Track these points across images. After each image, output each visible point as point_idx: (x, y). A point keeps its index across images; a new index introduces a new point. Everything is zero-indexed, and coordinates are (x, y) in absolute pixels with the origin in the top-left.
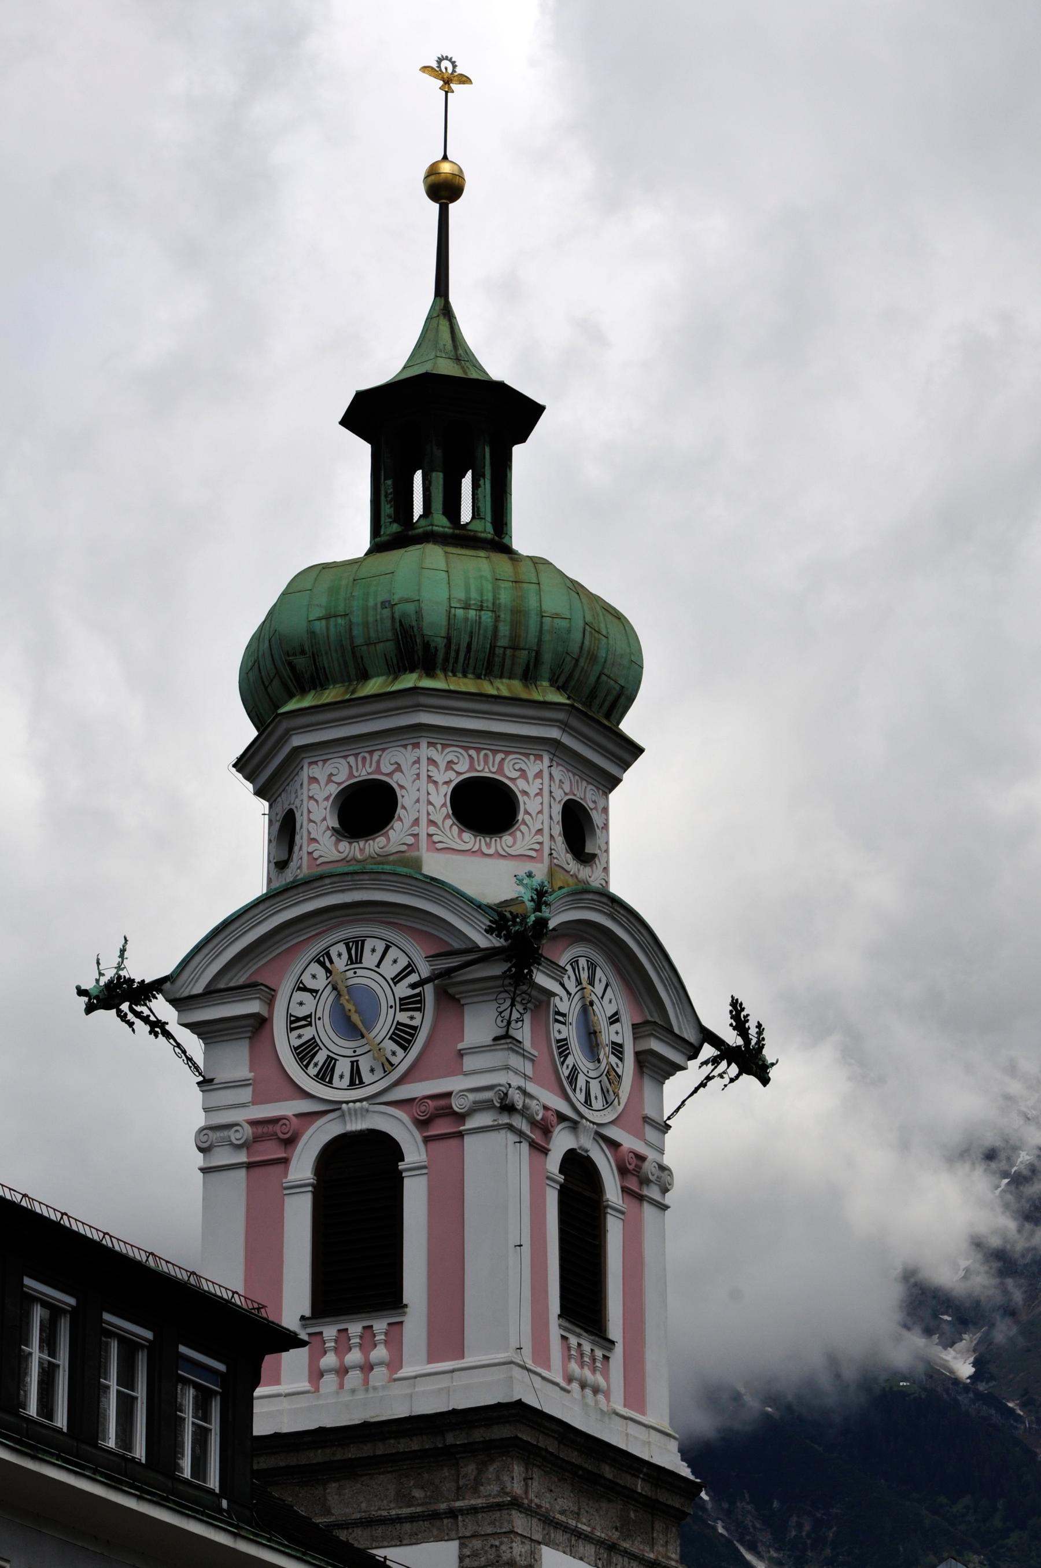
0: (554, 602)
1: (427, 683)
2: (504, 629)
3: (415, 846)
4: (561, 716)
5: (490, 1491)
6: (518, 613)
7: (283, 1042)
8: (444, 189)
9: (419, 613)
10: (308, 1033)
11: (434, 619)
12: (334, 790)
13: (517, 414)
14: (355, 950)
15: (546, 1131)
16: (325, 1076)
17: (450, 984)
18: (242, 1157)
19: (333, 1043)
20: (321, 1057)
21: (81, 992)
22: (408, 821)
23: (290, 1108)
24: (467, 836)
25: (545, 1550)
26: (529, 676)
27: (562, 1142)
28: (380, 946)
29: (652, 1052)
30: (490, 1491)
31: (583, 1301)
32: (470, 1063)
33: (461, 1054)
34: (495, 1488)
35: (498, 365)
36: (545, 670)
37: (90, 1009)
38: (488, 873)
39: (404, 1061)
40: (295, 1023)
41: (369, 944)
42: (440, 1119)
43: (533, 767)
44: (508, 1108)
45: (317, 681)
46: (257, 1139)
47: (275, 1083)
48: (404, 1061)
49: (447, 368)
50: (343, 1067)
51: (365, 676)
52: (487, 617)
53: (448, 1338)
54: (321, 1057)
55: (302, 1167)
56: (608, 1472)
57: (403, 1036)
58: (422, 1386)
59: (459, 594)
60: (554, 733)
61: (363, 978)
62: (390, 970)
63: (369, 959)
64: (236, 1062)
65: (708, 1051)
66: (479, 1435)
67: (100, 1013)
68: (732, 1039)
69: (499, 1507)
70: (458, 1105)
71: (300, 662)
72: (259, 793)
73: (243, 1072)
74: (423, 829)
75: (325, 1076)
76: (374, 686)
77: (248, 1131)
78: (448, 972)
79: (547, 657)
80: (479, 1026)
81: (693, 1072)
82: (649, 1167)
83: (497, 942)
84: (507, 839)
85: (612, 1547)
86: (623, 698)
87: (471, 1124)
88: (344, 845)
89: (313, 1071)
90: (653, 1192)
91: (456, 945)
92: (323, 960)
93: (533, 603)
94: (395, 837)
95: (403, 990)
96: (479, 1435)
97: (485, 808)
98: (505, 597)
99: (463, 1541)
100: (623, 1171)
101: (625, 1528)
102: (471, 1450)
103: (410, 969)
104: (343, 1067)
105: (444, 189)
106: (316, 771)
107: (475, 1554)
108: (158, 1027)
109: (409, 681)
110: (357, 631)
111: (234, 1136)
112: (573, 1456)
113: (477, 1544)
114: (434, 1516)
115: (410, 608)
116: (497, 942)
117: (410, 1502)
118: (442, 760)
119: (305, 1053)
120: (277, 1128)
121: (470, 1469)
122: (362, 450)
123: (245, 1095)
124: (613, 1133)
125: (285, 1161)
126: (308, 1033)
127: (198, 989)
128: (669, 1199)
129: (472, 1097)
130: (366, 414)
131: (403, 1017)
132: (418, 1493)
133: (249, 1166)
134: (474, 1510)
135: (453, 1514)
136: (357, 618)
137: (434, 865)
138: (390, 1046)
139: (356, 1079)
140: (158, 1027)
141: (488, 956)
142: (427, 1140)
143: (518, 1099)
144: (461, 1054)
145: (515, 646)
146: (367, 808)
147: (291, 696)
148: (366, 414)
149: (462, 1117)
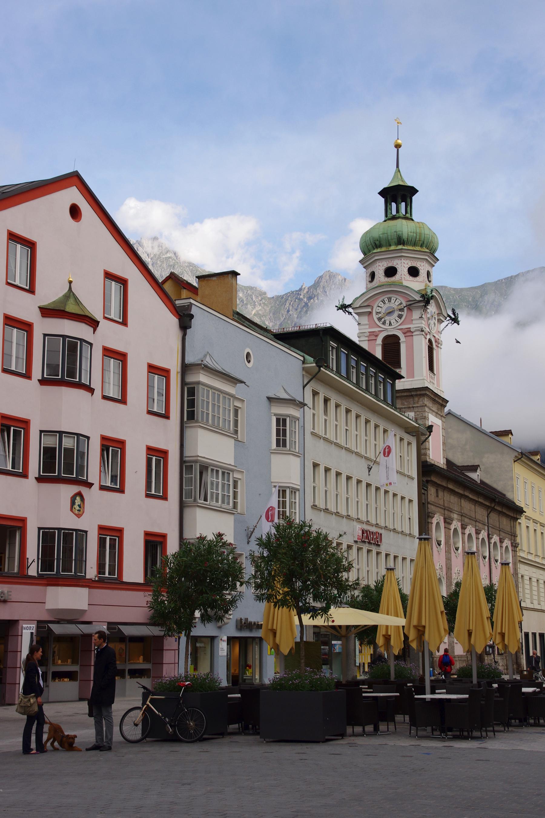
0: (427, 232)
1: (404, 248)
2: (418, 237)
3: (402, 279)
4: (428, 254)
5: (420, 403)
6: (420, 234)
7: (375, 317)
8: (398, 146)
9: (402, 234)
10: (380, 315)
12: (384, 268)
13: (413, 191)
14: (390, 299)
15: (427, 335)
16: (384, 323)
17: (411, 306)
18: (367, 339)
21: (336, 306)
22: (400, 275)
23: (377, 329)
24: (411, 277)
25: (430, 414)
26: (421, 246)
27: (428, 337)
28: (395, 299)
29: (440, 319)
30: (420, 403)
32: (414, 322)
33: (412, 320)
34: (422, 403)
35: (409, 183)
36: (425, 245)
37: (338, 310)
38: (416, 285)
39: (400, 321)
40: (377, 313)
41: (392, 298)
42: (408, 332)
43: (422, 264)
44: (422, 331)
45: (380, 246)
46: (370, 335)
47: (372, 324)
48: (400, 321)
49: (401, 183)
50: (388, 322)
51: (390, 246)
52: (415, 235)
53: (411, 374)
55: (379, 341)
56: (437, 399)
58: (406, 383)
59: (410, 230)
60: (427, 258)
62: (397, 303)
63: (393, 301)
64: (365, 320)
65: (448, 318)
66: (419, 393)
67: (340, 310)
68: (453, 316)
69: (423, 406)
70: (412, 330)
71: (377, 243)
72: (364, 267)
73: (367, 322)
74: (403, 276)
75: (384, 323)
76: (393, 248)
77: (368, 334)
78: (410, 305)
79: (425, 242)
80: (416, 314)
81: (446, 323)
82: (440, 341)
83: (421, 299)
84: (418, 278)
85: (437, 413)
86: (435, 251)
87: (414, 334)
89: (381, 322)
90: (439, 345)
91: (411, 299)
93: (423, 232)
94: (396, 278)
96: (419, 393)
97: (414, 272)
98: (418, 231)
99: (415, 412)
100: (436, 342)
101: (438, 409)
102: (416, 395)
103: (401, 304)
104: (388, 322)
105: (398, 146)
106: (380, 264)
107: (418, 415)
108: (350, 313)
109: (400, 247)
110: (389, 237)
111: (366, 335)
112: (432, 396)
113: (418, 413)
114: (409, 408)
115: (401, 233)
116: (421, 299)
117: (404, 405)
118: (406, 262)
119: (380, 319)
120: (374, 333)
121: (416, 399)
122: (383, 200)
123: (367, 327)
124: (435, 335)
125: (376, 340)
126: (380, 315)
127: (358, 306)
128: (442, 347)
129: (415, 329)
130: (384, 193)
131: (400, 313)
132: (406, 403)
133: (368, 340)
134: (418, 407)
135: (413, 407)
136: (389, 234)
137: (405, 283)
138: (397, 318)
140: (350, 313)
141: (419, 301)
142: (405, 336)
143: (424, 329)
144: (412, 320)
145: (420, 241)
146: (391, 272)
147: (374, 249)
148: (384, 193)
149: (413, 332)
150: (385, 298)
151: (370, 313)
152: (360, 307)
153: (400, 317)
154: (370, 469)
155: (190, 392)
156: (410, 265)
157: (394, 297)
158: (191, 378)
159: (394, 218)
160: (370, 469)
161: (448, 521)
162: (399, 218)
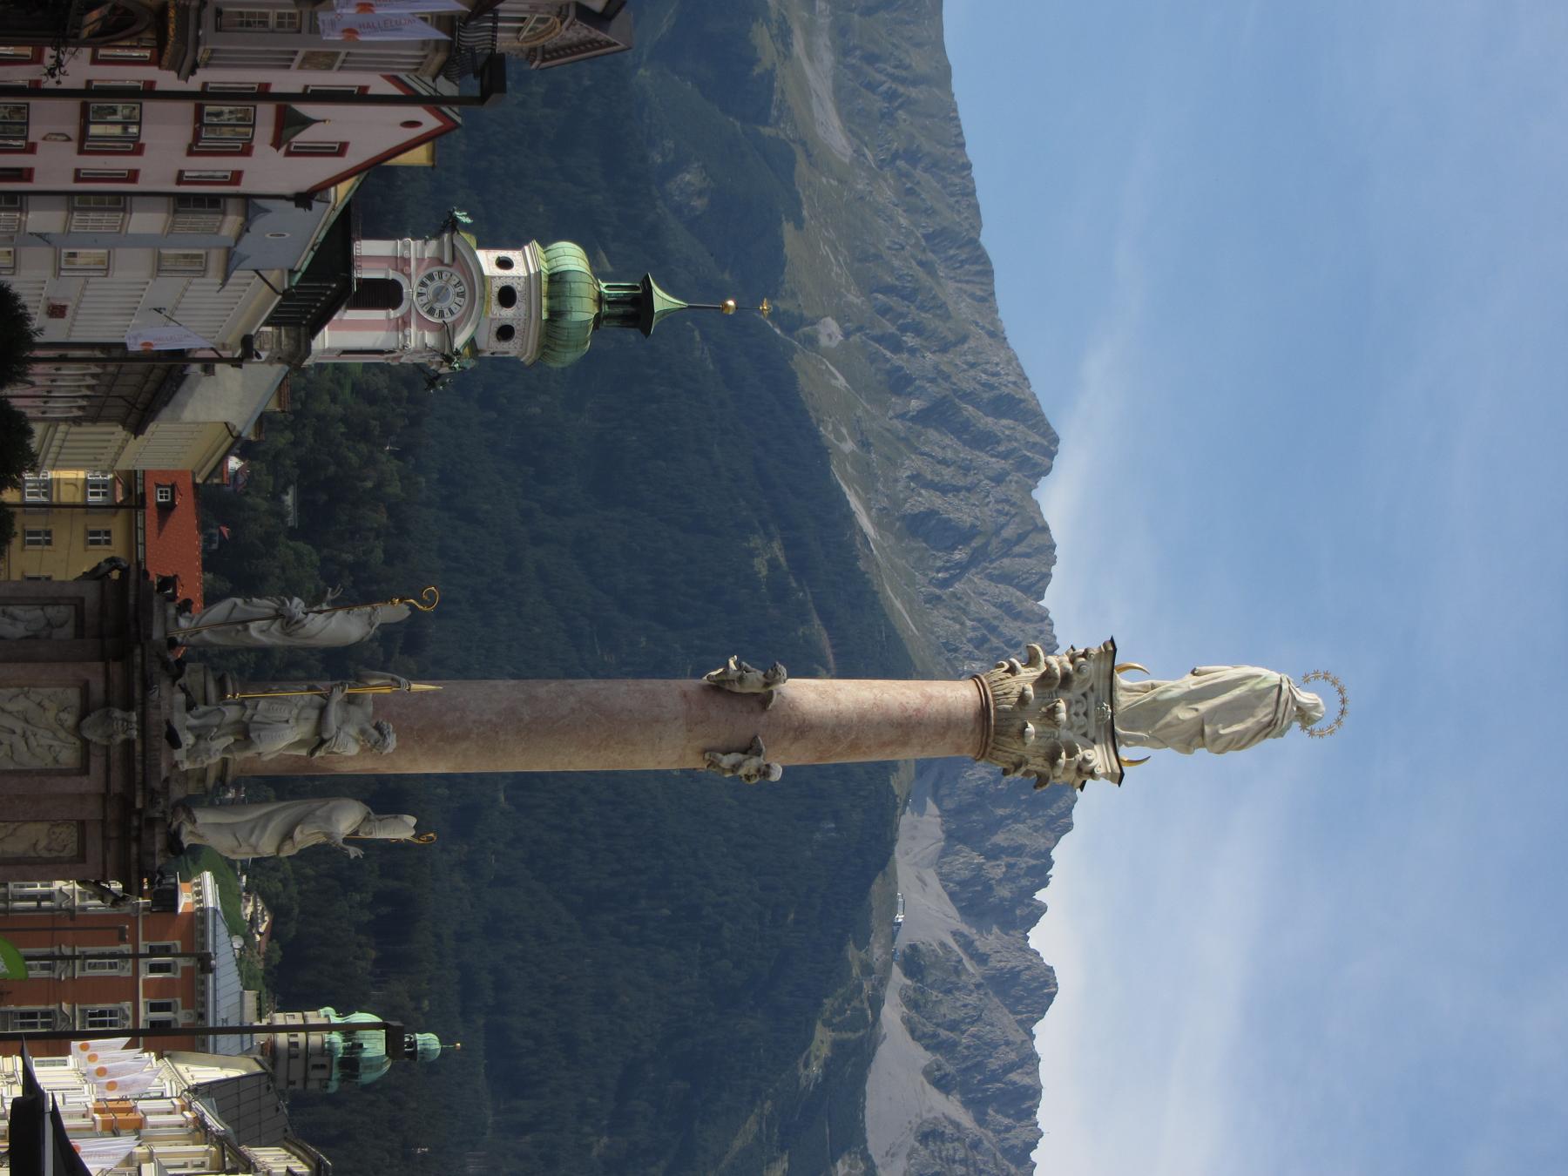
7: (435, 270)
11: (563, 324)
16: (423, 284)
19: (433, 286)
31: (346, 352)
40: (440, 273)
42: (404, 323)
55: (392, 275)
88: (496, 290)
92: (460, 283)
104: (424, 290)
109: (545, 316)
119: (430, 277)
141: (451, 346)
151: (441, 262)
152: (453, 246)
153: (431, 311)
154: (159, 310)
155: (213, 203)
156: (516, 328)
157: (464, 302)
158: (231, 204)
159: (600, 300)
160: (159, 310)
161: (94, 376)
162: (600, 308)
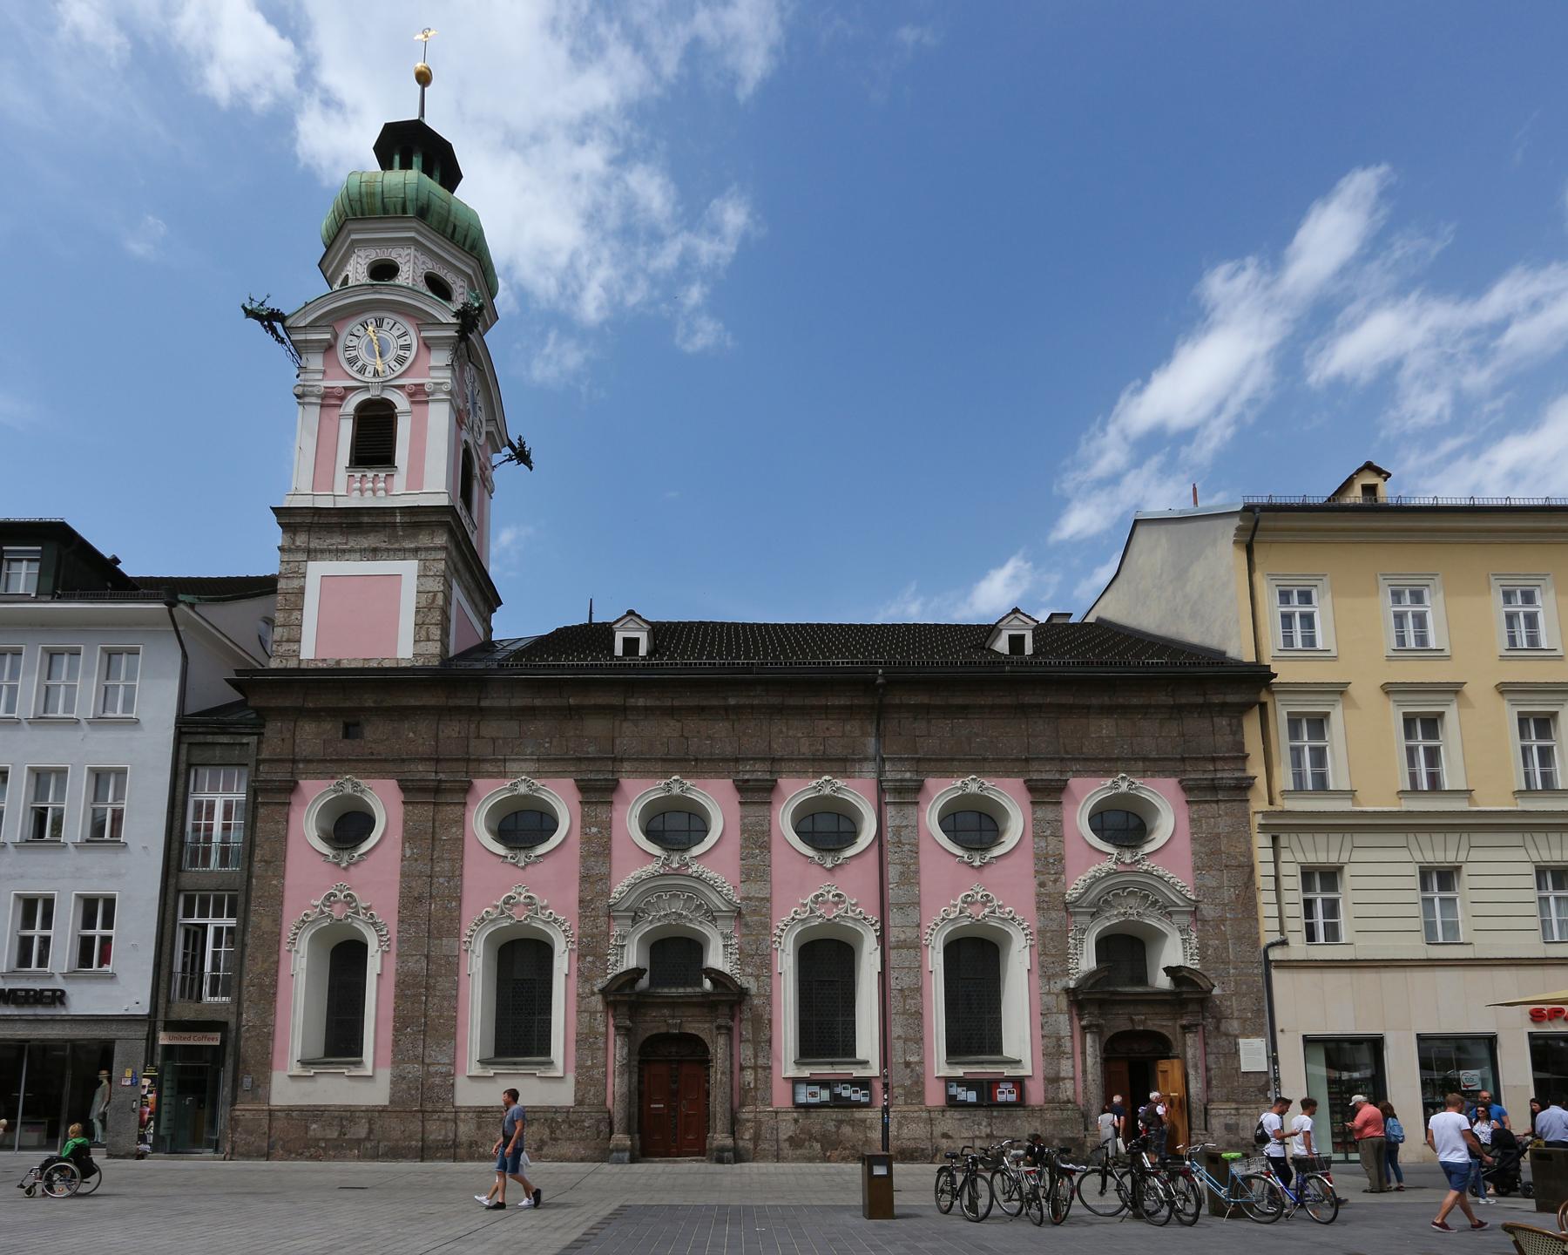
19: (364, 357)
20: (360, 364)
40: (347, 348)
48: (399, 370)
50: (370, 369)
54: (360, 364)
57: (400, 360)
61: (382, 334)
75: (362, 370)
92: (364, 325)
95: (401, 342)
106: (362, 253)
126: (354, 353)
134: (427, 549)
138: (393, 363)
139: (376, 373)
150: (370, 318)
